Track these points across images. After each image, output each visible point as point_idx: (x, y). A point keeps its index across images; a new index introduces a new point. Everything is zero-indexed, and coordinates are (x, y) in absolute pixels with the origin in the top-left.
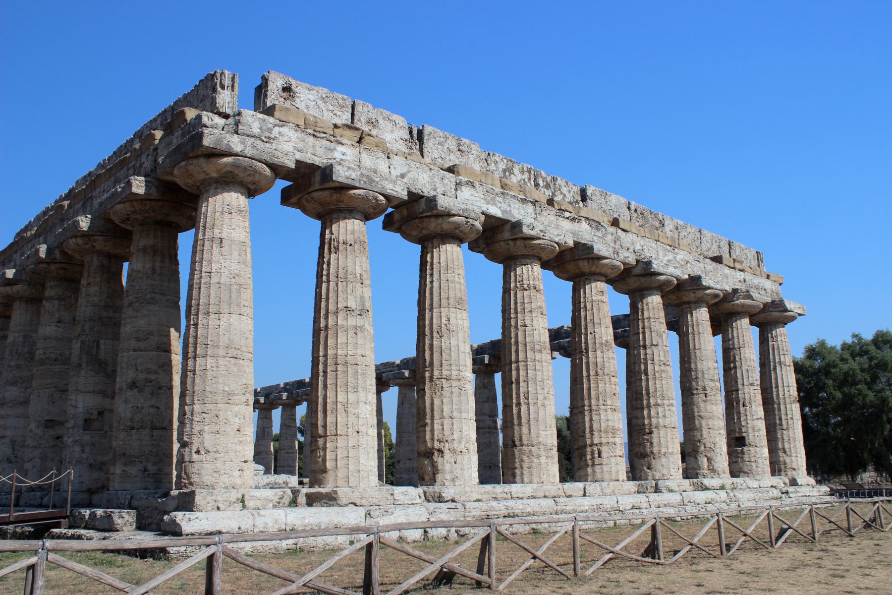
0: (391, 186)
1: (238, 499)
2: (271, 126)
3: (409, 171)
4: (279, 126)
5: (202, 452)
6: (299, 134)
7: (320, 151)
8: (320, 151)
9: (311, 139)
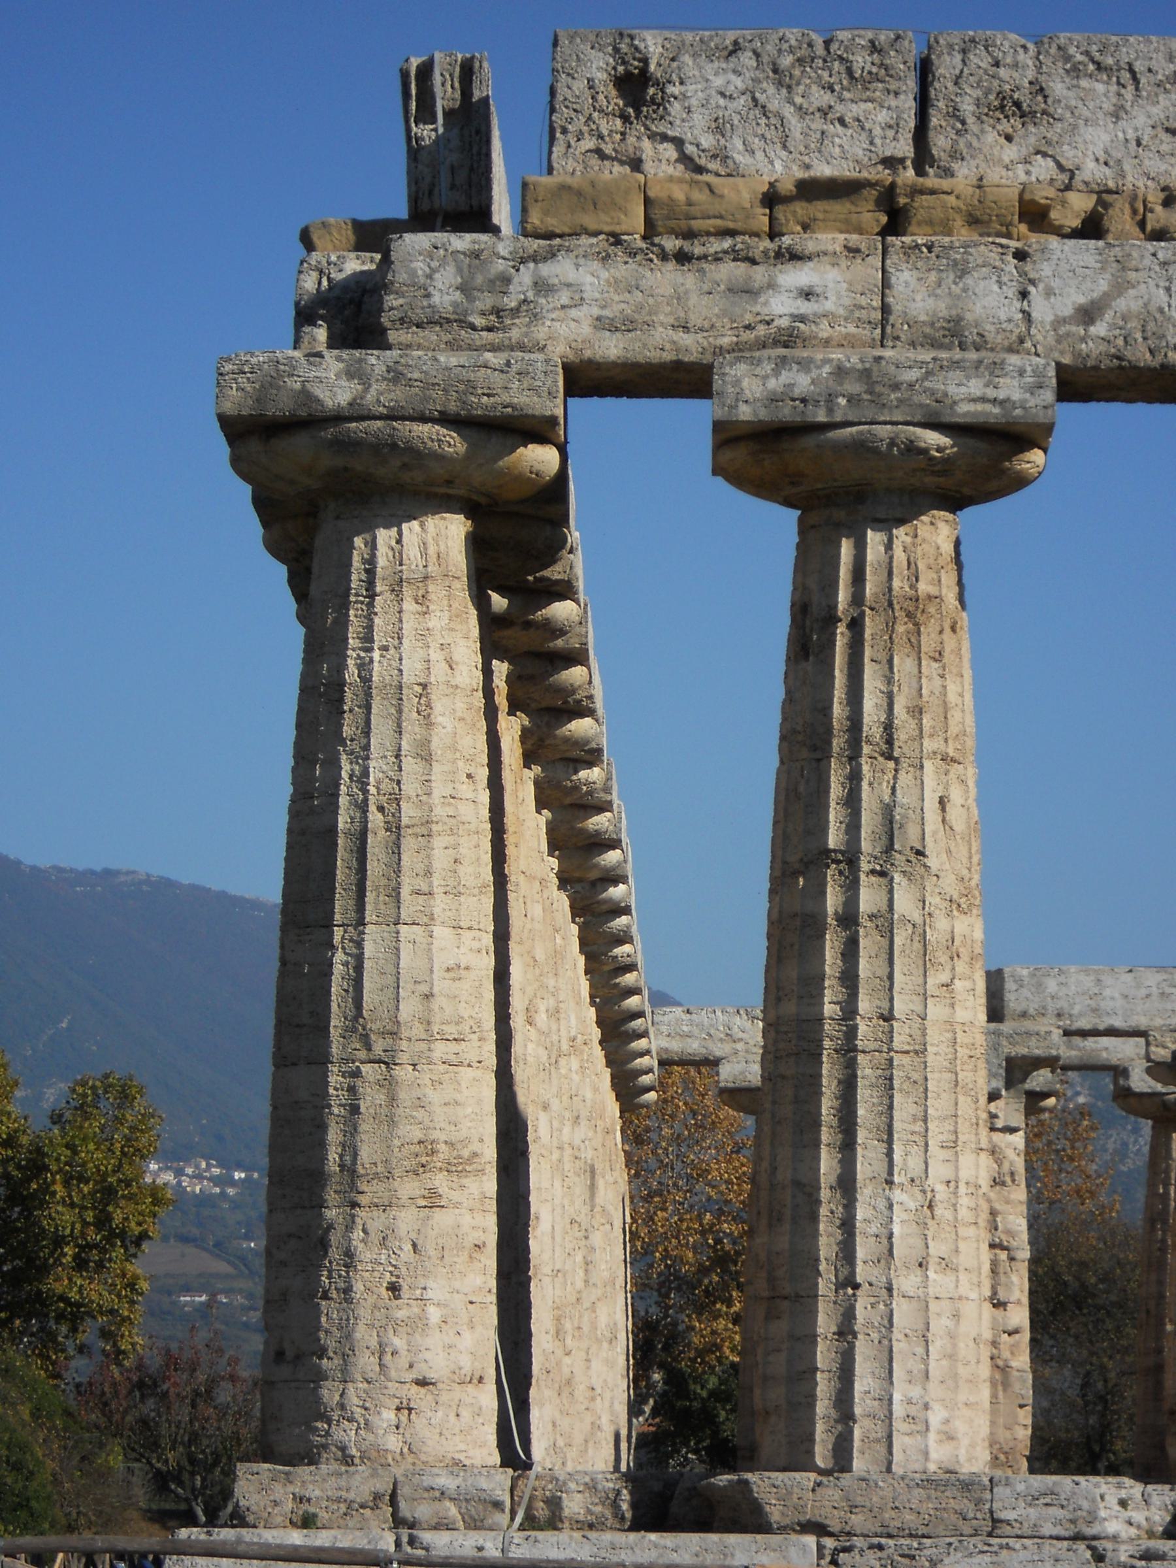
0: (975, 387)
1: (377, 1497)
2: (500, 266)
3: (1120, 287)
4: (535, 258)
5: (290, 1354)
6: (623, 268)
7: (701, 308)
8: (701, 308)
9: (665, 279)
